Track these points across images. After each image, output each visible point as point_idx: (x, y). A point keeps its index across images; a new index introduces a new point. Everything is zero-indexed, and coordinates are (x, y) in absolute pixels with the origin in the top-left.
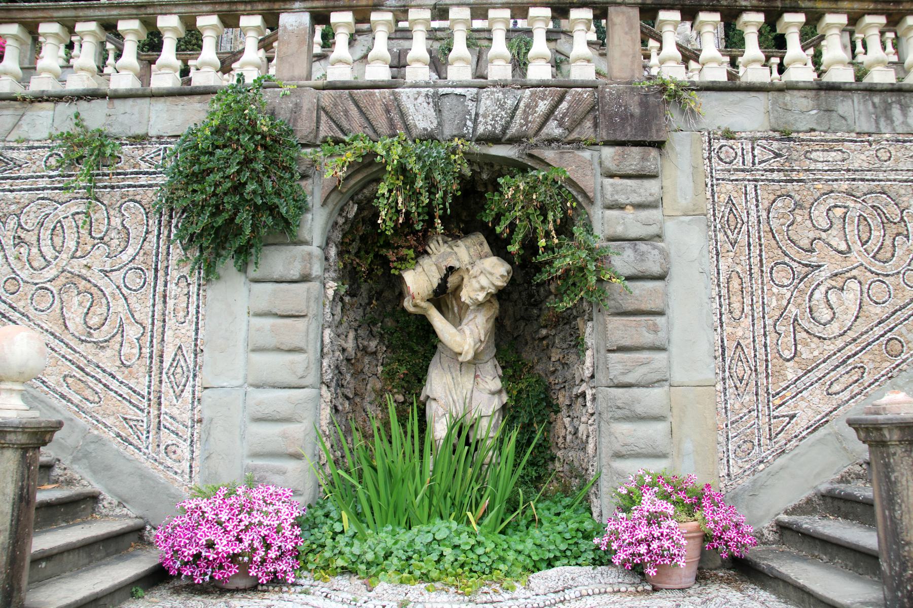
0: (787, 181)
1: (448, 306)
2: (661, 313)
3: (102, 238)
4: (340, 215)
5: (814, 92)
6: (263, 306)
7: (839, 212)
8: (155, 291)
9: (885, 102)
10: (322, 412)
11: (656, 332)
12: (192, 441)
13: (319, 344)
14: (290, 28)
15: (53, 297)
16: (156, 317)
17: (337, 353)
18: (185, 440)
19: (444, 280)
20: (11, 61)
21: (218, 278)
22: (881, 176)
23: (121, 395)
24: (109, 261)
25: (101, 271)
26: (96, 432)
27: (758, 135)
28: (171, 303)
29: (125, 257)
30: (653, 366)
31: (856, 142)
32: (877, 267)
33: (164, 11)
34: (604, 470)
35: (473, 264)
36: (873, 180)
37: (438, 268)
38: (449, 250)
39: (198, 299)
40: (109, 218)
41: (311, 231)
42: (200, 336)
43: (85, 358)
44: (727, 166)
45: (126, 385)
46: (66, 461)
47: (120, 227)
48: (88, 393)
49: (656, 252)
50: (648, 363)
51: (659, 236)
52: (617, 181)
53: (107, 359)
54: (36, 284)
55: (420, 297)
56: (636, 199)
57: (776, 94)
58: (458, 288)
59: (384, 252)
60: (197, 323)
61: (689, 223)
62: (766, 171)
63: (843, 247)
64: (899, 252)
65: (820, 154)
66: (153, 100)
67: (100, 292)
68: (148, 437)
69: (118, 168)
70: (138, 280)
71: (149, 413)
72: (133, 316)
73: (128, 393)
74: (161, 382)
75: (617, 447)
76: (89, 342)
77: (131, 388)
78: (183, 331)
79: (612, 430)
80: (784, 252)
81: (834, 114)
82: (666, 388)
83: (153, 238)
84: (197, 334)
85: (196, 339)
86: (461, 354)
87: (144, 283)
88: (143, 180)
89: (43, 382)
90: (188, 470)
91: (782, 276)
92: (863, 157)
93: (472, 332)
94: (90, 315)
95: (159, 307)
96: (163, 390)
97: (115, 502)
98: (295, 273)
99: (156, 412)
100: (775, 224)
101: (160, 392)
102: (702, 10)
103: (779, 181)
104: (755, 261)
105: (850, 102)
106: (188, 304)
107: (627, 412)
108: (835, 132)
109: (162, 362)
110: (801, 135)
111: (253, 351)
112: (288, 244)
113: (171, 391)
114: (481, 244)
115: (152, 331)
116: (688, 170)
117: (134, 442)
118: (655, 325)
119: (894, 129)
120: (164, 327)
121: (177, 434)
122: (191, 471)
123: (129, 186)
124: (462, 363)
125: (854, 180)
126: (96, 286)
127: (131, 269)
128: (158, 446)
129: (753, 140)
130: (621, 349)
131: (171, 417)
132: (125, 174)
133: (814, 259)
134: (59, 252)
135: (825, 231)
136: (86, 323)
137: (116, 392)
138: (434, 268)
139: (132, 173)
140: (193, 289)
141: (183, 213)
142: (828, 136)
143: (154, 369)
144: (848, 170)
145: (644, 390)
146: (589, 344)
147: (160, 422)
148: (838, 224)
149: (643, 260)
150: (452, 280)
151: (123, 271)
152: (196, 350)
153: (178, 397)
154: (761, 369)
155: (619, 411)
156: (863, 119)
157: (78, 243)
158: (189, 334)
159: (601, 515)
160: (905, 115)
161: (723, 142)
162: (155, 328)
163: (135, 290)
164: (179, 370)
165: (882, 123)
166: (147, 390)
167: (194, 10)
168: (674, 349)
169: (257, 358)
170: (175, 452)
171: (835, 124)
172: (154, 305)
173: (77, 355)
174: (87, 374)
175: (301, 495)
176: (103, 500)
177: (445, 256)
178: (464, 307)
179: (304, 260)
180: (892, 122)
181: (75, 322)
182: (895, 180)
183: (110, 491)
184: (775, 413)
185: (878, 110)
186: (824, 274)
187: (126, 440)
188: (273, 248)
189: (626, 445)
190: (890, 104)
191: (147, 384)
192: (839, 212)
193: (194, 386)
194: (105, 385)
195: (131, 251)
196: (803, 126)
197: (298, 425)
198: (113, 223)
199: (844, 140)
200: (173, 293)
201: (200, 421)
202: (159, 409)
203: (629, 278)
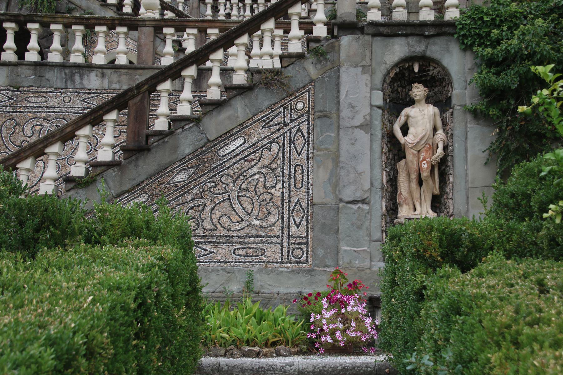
0: (13, 112)
5: (34, 67)
9: (72, 72)
22: (64, 110)
31: (54, 92)
36: (59, 112)
57: (13, 67)
62: (3, 106)
65: (33, 99)
81: (44, 78)
92: (56, 100)
103: (9, 112)
105: (53, 72)
108: (43, 87)
110: (25, 89)
119: (75, 87)
125: (49, 112)
135: (29, 137)
142: (40, 90)
144: (47, 107)
156: (58, 81)
165: (69, 83)
180: (74, 82)
182: (71, 112)
185: (68, 77)
190: (74, 74)
192: (38, 128)
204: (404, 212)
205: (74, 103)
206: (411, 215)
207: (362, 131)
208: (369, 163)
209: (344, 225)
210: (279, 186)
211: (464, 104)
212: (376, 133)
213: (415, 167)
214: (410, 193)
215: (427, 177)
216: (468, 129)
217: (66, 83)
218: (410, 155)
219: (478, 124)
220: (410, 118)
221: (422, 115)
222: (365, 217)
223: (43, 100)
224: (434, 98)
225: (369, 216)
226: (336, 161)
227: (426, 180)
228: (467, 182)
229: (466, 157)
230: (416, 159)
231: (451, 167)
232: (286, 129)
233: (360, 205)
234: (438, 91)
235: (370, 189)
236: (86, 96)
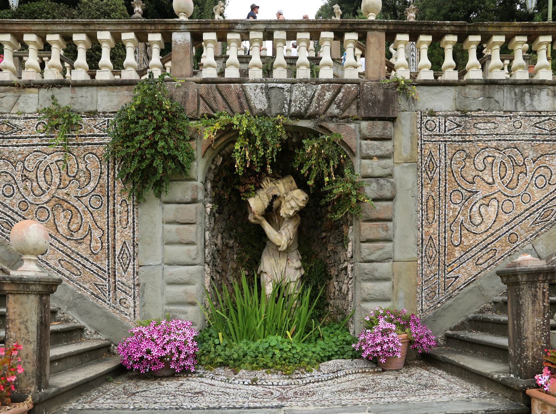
1: (272, 219)
2: (390, 220)
3: (74, 177)
4: (212, 163)
6: (171, 217)
7: (490, 160)
8: (108, 209)
10: (206, 279)
11: (387, 231)
12: (134, 296)
13: (203, 240)
14: (179, 43)
15: (49, 212)
16: (110, 224)
17: (213, 246)
18: (130, 296)
19: (271, 203)
20: (8, 60)
21: (145, 201)
22: (515, 137)
23: (92, 271)
24: (80, 191)
25: (76, 197)
26: (80, 292)
27: (449, 113)
28: (118, 216)
29: (89, 188)
30: (385, 250)
31: (503, 117)
32: (508, 192)
33: (101, 28)
34: (357, 309)
35: (287, 194)
36: (510, 140)
37: (268, 196)
38: (274, 185)
39: (133, 214)
40: (78, 164)
41: (196, 172)
42: (136, 236)
43: (70, 249)
44: (430, 133)
45: (95, 265)
46: (64, 310)
47: (85, 170)
48: (73, 269)
49: (389, 184)
50: (382, 248)
51: (391, 175)
52: (369, 142)
53: (82, 249)
54: (38, 205)
55: (257, 213)
56: (379, 153)
58: (279, 208)
59: (237, 187)
60: (134, 228)
61: (407, 167)
62: (451, 135)
63: (490, 180)
64: (520, 183)
65: (482, 125)
66: (99, 88)
67: (76, 210)
68: (109, 295)
69: (81, 132)
70: (98, 203)
71: (109, 280)
72: (96, 224)
73: (96, 270)
74: (115, 263)
75: (364, 295)
76: (72, 240)
77: (98, 267)
78: (126, 233)
79: (362, 286)
80: (458, 184)
82: (391, 263)
83: (105, 176)
84: (134, 234)
85: (134, 238)
86: (280, 246)
87: (102, 204)
88: (96, 140)
89: (47, 264)
90: (133, 313)
91: (456, 198)
92: (506, 126)
93: (286, 234)
94: (71, 223)
95: (111, 219)
96: (116, 267)
97: (93, 331)
98: (188, 198)
99: (113, 280)
100: (454, 167)
101: (115, 268)
102: (422, 34)
103: (458, 142)
104: (442, 189)
106: (128, 217)
107: (370, 276)
108: (492, 111)
109: (115, 251)
110: (473, 114)
111: (166, 244)
112: (184, 181)
113: (121, 268)
114: (291, 182)
115: (108, 233)
116: (409, 135)
117: (102, 297)
118: (387, 226)
120: (115, 230)
121: (126, 293)
122: (135, 314)
123: (88, 144)
124: (280, 252)
125: (500, 140)
126: (73, 206)
127: (93, 196)
128: (116, 299)
129: (446, 116)
130: (369, 241)
131: (122, 283)
132: (86, 136)
133: (474, 188)
134: (50, 185)
135: (481, 171)
136: (69, 228)
137: (89, 269)
138: (265, 196)
139: (89, 136)
140: (130, 208)
141: (121, 162)
142: (488, 114)
143: (110, 255)
144: (497, 134)
145: (380, 264)
146: (351, 239)
147: (115, 286)
148: (489, 167)
149: (382, 189)
150: (276, 203)
151: (89, 197)
152: (134, 244)
153: (125, 271)
154: (442, 251)
155: (366, 276)
157: (61, 179)
158: (129, 234)
159: (354, 333)
161: (429, 118)
162: (110, 231)
163: (96, 209)
164: (125, 256)
166: (107, 268)
167: (119, 28)
168: (396, 241)
169: (169, 248)
170: (125, 303)
171: (492, 106)
172: (108, 218)
173: (66, 248)
174: (72, 259)
175: (196, 325)
176: (86, 330)
177: (271, 189)
178: (281, 219)
179: (193, 190)
181: (63, 228)
182: (522, 140)
183: (90, 326)
184: (448, 276)
186: (479, 196)
187: (97, 297)
188: (175, 182)
189: (369, 294)
191: (107, 264)
192: (490, 160)
193: (134, 265)
194: (83, 265)
195: (92, 184)
196: (474, 107)
197: (193, 286)
198: (80, 167)
199: (496, 116)
200: (119, 210)
201: (138, 285)
202: (115, 279)
203: (375, 200)
205: (525, 128)
217: (516, 105)
223: (493, 127)
236: (537, 120)
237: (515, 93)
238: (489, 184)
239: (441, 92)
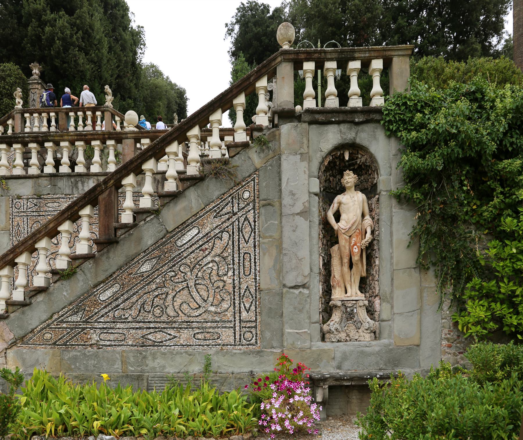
0: (38, 216)
9: (76, 180)
27: (30, 197)
44: (18, 210)
65: (51, 204)
81: (57, 187)
116: (4, 212)
142: (55, 196)
160: (83, 186)
161: (17, 200)
171: (57, 191)
180: (78, 189)
190: (78, 181)
196: (45, 192)
199: (60, 198)
204: (337, 294)
206: (343, 297)
207: (302, 218)
208: (308, 249)
209: (287, 309)
210: (230, 273)
211: (390, 189)
212: (314, 220)
213: (347, 251)
214: (342, 276)
215: (357, 261)
216: (393, 214)
217: (72, 190)
218: (343, 240)
219: (402, 209)
220: (342, 205)
221: (353, 202)
222: (306, 301)
223: (57, 205)
224: (360, 186)
225: (309, 300)
226: (280, 248)
227: (357, 264)
228: (392, 264)
229: (391, 241)
230: (348, 243)
231: (377, 250)
232: (234, 218)
233: (301, 290)
234: (364, 179)
235: (310, 274)
237: (71, 182)
238: (55, 244)
239: (24, 183)
